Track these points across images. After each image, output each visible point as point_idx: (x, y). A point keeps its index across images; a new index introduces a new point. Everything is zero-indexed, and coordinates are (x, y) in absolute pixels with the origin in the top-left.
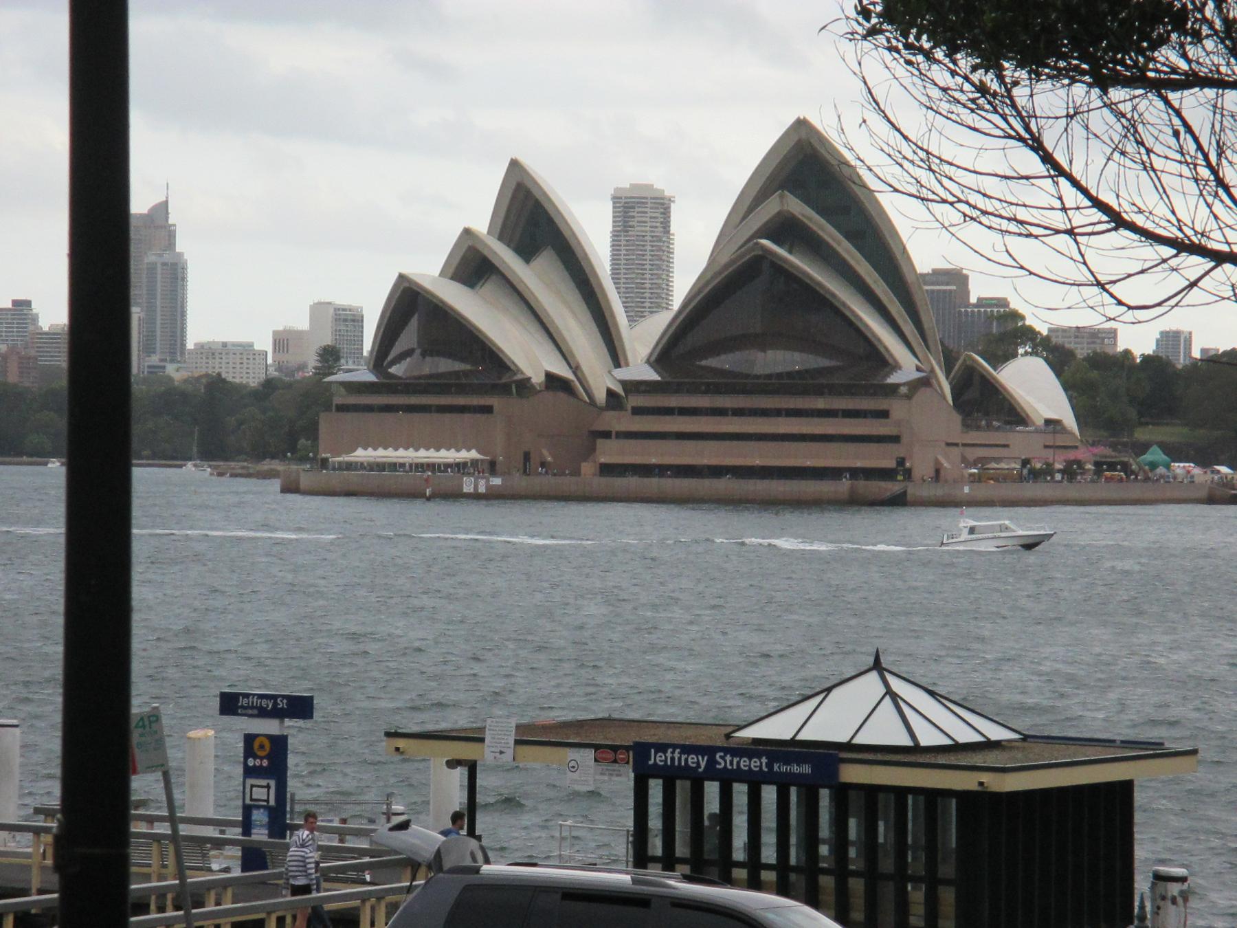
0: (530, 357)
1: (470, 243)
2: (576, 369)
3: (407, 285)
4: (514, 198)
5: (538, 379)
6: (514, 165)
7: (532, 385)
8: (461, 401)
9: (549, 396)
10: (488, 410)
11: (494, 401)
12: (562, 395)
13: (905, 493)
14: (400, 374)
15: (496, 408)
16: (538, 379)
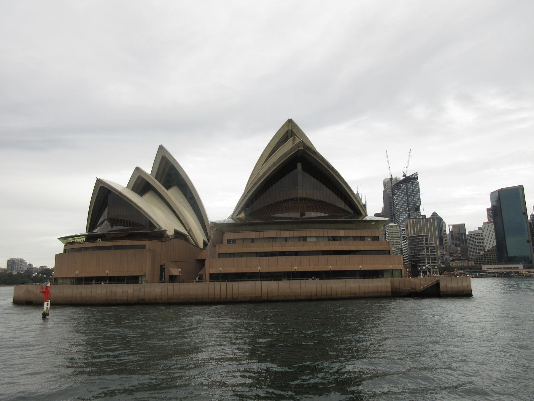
0: (166, 222)
1: (139, 174)
2: (189, 231)
3: (101, 185)
4: (160, 164)
5: (170, 232)
6: (161, 148)
7: (168, 236)
8: (128, 243)
9: (176, 242)
10: (143, 247)
11: (146, 242)
12: (182, 241)
13: (438, 284)
14: (99, 233)
15: (147, 247)
16: (170, 232)
